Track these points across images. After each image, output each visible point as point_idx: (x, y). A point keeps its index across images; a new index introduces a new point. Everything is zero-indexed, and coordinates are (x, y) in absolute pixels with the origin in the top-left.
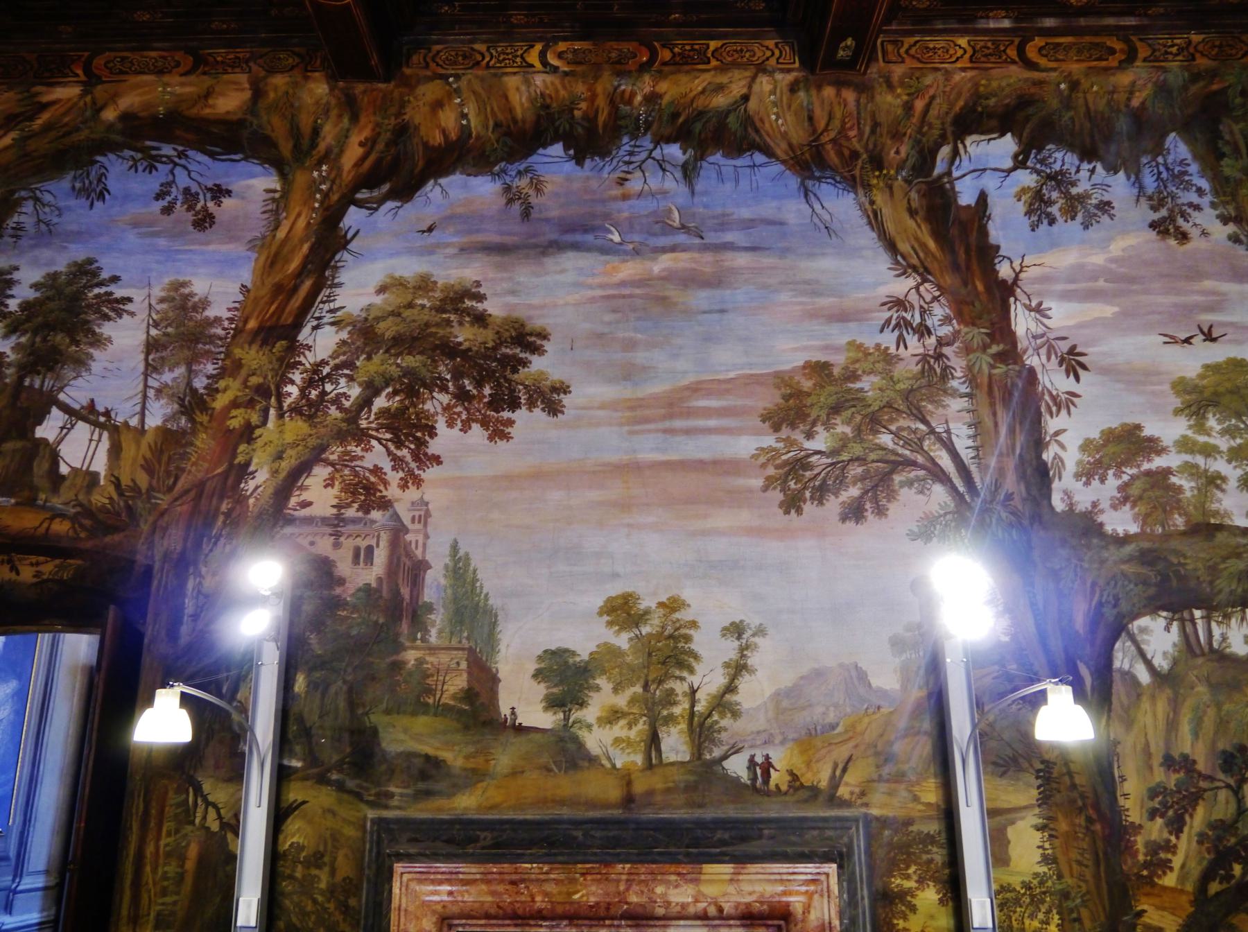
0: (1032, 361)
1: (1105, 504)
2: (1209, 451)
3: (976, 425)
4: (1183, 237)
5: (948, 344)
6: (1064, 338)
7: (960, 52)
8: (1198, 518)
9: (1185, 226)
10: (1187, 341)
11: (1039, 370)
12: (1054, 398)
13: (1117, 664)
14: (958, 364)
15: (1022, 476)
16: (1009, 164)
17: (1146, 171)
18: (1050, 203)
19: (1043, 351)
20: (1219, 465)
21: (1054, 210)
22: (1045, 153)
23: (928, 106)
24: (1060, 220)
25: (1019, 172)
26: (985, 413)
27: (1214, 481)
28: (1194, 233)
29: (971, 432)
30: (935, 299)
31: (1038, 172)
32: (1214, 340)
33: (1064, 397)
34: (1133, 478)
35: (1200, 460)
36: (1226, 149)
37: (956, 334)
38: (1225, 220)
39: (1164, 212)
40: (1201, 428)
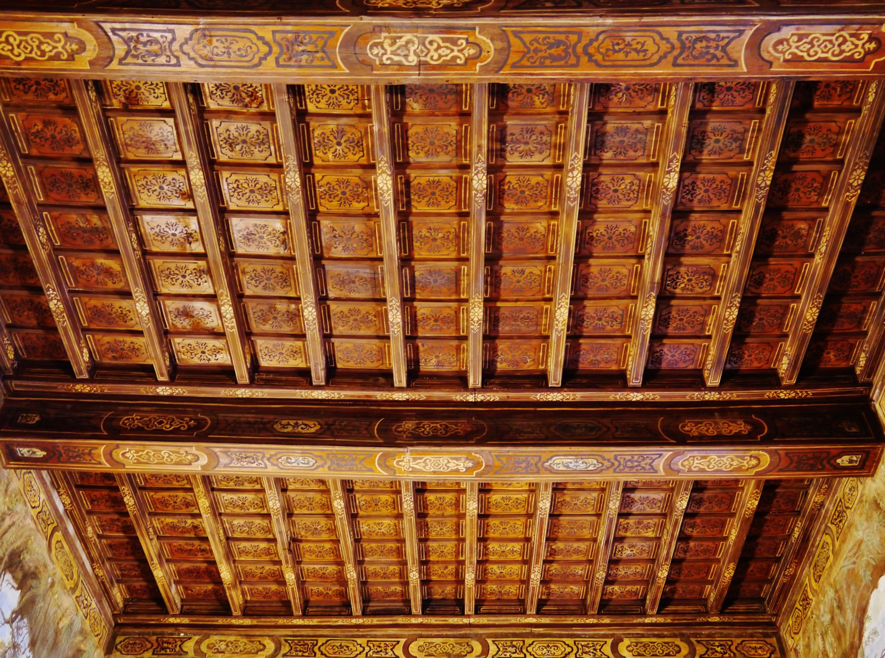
7: (37, 504)
16: (8, 616)
22: (21, 624)
23: (10, 527)
25: (7, 626)
31: (13, 637)
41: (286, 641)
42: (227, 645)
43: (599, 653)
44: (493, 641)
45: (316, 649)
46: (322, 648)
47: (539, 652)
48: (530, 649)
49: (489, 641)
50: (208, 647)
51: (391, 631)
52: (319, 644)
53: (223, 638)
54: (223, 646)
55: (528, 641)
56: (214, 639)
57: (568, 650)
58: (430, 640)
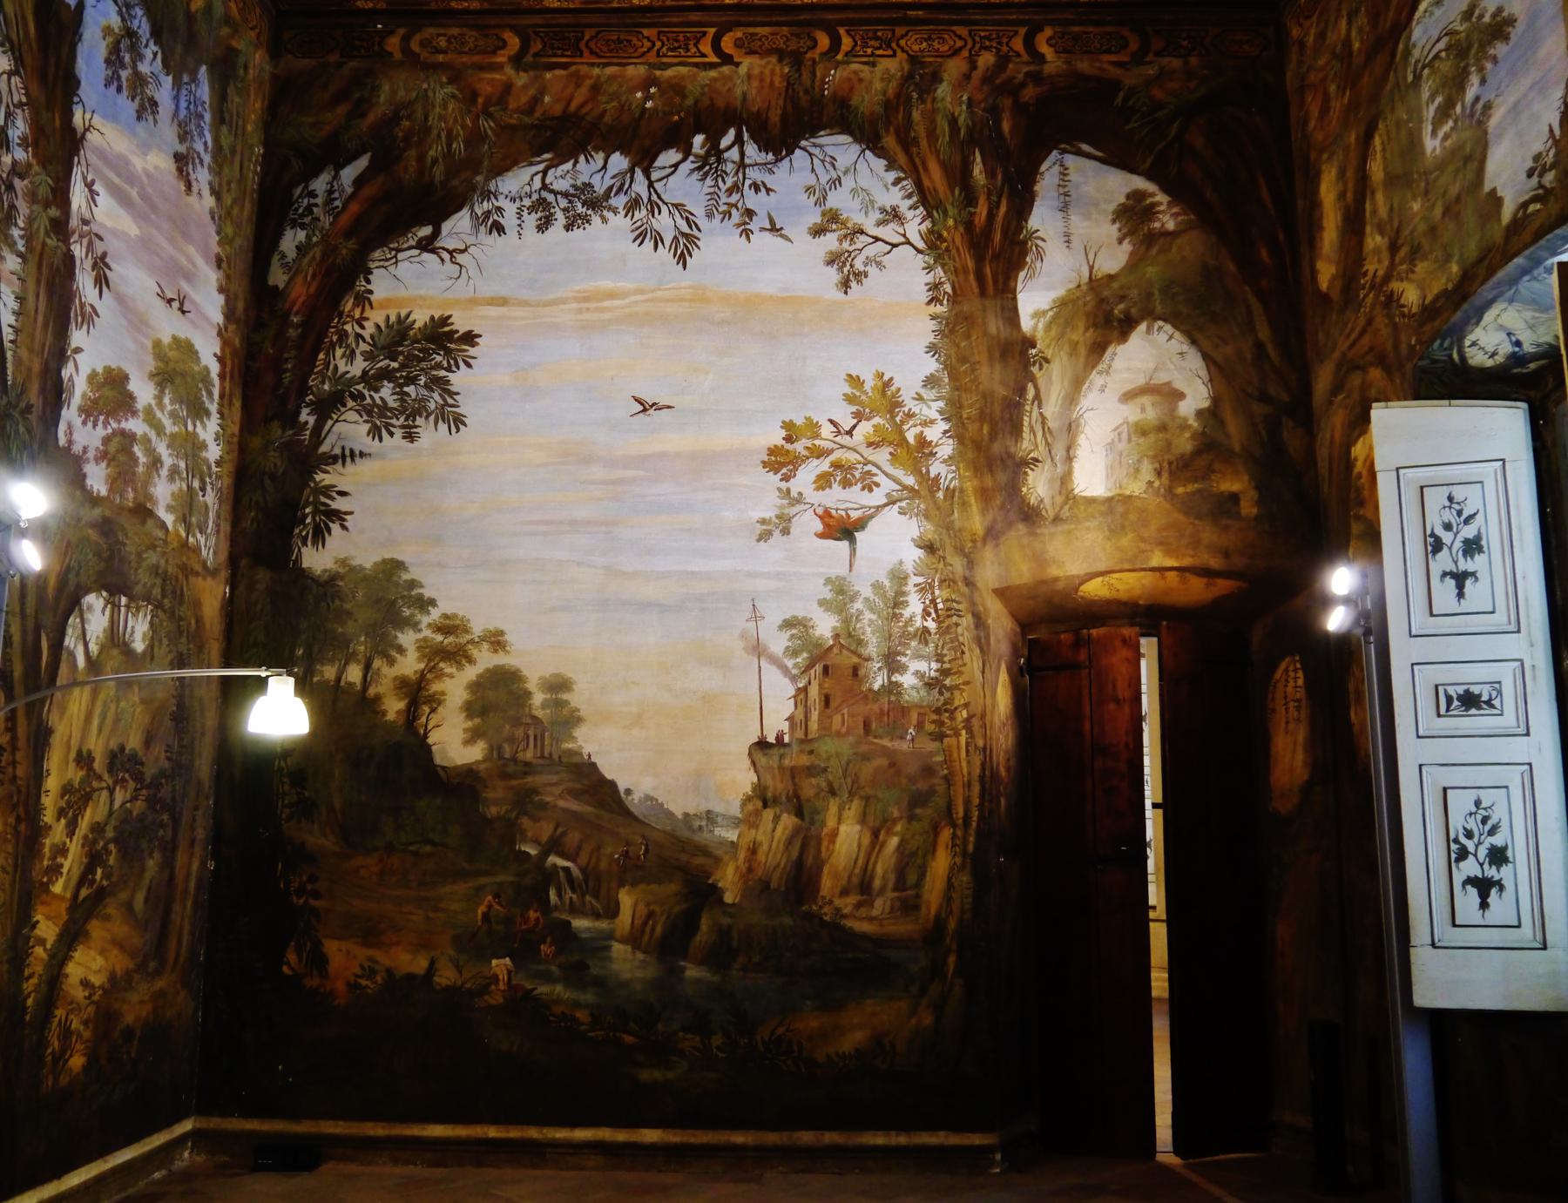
0: (78, 250)
1: (91, 454)
2: (159, 429)
3: (20, 299)
4: (189, 186)
5: (22, 178)
6: (101, 239)
8: (141, 499)
9: (192, 177)
10: (170, 301)
11: (78, 263)
12: (82, 306)
13: (67, 642)
14: (23, 207)
15: (43, 390)
17: (184, 92)
18: (123, 66)
19: (85, 241)
20: (162, 449)
21: (124, 74)
24: (125, 92)
26: (31, 286)
27: (156, 462)
28: (195, 188)
29: (16, 306)
30: (20, 105)
31: (123, 20)
32: (184, 312)
33: (88, 309)
34: (114, 432)
35: (152, 435)
36: (227, 116)
37: (29, 165)
38: (213, 192)
39: (182, 149)
40: (159, 398)
41: (537, 34)
42: (448, 41)
43: (1005, 49)
44: (848, 32)
45: (582, 45)
46: (592, 45)
47: (916, 48)
48: (902, 42)
49: (842, 31)
50: (421, 44)
51: (695, 17)
52: (587, 37)
53: (442, 31)
54: (443, 43)
55: (900, 31)
56: (429, 32)
57: (959, 43)
58: (751, 30)
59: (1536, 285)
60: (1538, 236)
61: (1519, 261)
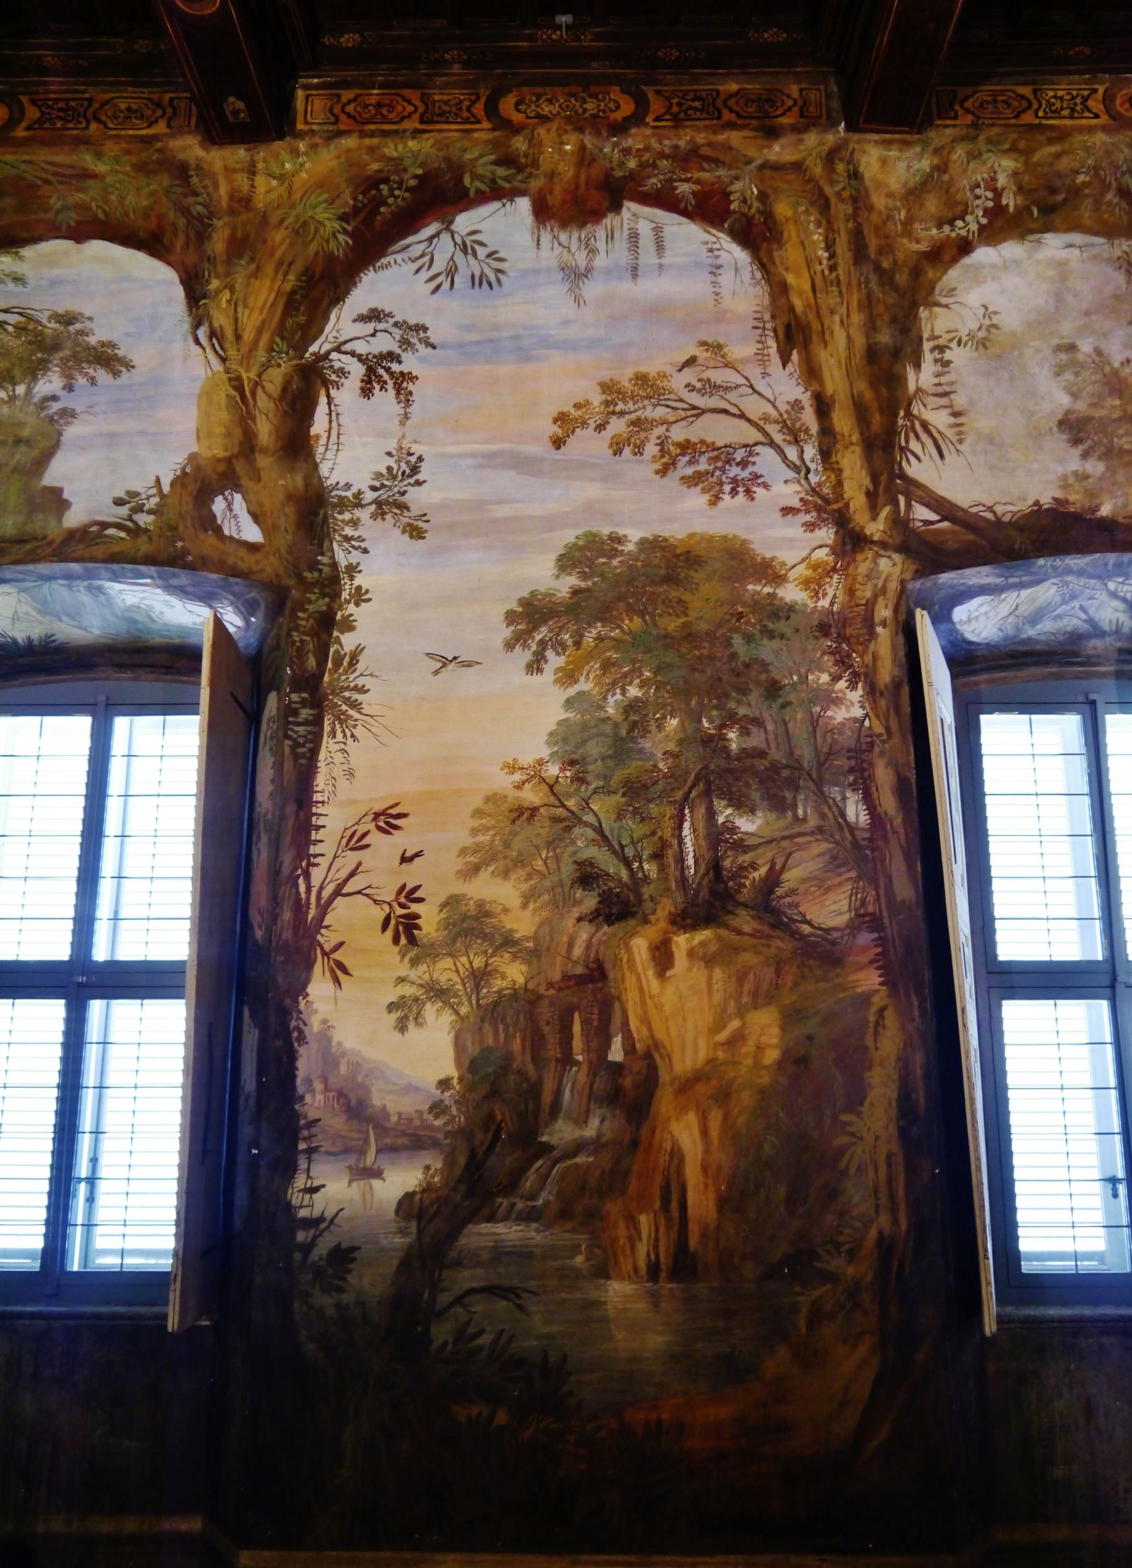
59: (64, 592)
60: (112, 559)
61: (75, 567)
